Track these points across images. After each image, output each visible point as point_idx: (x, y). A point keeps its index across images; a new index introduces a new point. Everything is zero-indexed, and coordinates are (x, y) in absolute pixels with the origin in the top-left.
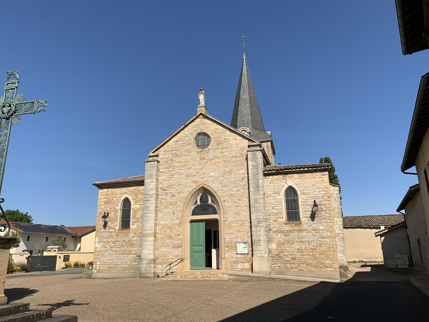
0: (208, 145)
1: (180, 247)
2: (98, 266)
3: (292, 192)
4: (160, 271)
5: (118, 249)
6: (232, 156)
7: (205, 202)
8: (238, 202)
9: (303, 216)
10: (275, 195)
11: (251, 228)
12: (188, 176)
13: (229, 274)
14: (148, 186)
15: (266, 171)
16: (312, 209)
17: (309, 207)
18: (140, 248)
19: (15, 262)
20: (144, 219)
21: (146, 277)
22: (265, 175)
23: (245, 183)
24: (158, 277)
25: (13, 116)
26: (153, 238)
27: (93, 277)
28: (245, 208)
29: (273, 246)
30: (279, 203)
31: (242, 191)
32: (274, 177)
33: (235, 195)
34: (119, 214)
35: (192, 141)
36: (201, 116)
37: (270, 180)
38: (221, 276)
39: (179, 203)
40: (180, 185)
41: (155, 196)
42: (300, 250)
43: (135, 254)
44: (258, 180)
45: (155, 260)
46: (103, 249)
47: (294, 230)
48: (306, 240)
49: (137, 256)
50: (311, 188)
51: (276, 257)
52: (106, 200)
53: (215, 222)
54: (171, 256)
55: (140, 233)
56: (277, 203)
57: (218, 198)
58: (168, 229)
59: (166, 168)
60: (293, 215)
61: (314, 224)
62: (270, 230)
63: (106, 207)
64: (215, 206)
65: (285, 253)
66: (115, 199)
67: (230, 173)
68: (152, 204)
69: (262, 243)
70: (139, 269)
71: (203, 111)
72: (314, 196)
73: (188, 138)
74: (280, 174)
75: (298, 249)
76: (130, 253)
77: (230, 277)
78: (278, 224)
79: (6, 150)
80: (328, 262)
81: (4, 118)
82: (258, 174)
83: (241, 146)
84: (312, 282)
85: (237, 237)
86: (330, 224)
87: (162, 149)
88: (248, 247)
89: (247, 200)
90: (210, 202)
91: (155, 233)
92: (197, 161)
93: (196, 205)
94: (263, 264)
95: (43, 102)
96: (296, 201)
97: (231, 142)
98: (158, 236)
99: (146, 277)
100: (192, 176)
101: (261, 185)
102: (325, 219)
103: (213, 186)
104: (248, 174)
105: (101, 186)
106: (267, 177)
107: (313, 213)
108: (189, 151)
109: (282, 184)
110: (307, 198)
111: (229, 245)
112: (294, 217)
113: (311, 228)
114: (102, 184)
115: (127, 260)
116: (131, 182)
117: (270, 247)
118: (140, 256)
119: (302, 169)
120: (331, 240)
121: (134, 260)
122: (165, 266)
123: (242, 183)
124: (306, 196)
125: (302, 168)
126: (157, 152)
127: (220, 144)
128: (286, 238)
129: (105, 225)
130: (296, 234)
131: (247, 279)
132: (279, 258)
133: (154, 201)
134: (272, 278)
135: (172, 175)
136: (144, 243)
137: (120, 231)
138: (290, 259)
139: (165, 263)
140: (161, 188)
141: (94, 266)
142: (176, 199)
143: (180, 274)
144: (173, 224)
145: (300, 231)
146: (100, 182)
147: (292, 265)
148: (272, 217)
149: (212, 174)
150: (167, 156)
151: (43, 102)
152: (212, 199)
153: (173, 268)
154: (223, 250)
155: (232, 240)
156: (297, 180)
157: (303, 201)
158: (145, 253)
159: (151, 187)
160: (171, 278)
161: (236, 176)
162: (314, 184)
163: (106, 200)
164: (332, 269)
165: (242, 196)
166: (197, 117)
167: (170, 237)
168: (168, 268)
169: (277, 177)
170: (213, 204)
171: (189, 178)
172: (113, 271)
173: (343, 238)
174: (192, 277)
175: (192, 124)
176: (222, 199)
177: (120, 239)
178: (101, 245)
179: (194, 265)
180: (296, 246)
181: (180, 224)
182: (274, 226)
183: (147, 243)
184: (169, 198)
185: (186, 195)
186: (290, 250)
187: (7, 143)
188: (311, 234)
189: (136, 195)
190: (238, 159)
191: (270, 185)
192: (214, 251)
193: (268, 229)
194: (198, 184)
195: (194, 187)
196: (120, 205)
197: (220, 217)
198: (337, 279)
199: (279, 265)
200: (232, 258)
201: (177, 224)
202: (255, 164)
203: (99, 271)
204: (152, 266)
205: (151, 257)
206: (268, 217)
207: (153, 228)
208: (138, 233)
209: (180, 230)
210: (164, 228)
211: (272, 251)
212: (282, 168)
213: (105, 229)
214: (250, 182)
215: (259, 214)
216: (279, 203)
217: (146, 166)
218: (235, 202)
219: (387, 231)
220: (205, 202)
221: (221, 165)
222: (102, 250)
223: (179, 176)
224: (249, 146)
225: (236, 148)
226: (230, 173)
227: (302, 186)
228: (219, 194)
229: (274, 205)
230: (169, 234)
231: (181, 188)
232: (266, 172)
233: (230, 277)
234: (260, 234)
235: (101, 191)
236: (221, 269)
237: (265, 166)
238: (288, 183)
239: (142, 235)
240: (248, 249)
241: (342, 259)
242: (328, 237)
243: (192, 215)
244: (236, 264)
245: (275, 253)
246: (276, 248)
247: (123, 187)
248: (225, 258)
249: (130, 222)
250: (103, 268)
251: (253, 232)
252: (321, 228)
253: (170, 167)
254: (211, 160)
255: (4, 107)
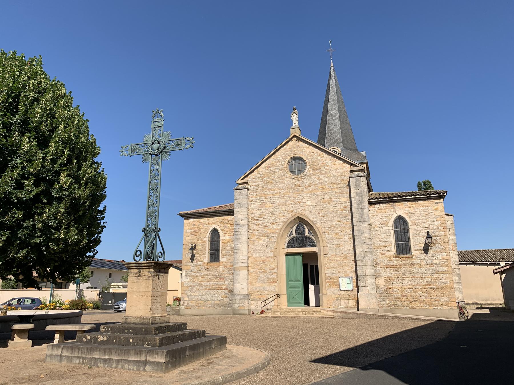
0: (303, 170)
1: (276, 282)
2: (186, 303)
3: (402, 222)
4: (254, 308)
5: (207, 284)
6: (332, 183)
7: (302, 233)
8: (340, 234)
9: (415, 248)
10: (382, 226)
11: (355, 262)
12: (281, 205)
13: (333, 311)
14: (239, 216)
15: (372, 199)
16: (425, 241)
17: (421, 238)
18: (231, 283)
19: (87, 298)
20: (236, 251)
21: (240, 314)
22: (370, 203)
23: (347, 213)
24: (253, 313)
25: (163, 153)
26: (245, 272)
27: (181, 313)
28: (348, 240)
29: (381, 282)
30: (388, 234)
31: (344, 221)
32: (381, 205)
33: (336, 226)
34: (207, 246)
35: (285, 166)
36: (294, 139)
37: (376, 209)
38: (325, 313)
39: (272, 235)
40: (273, 214)
41: (246, 226)
42: (411, 286)
43: (226, 289)
44: (363, 209)
45: (248, 296)
46: (191, 284)
47: (405, 264)
48: (418, 275)
49: (229, 292)
50: (424, 218)
51: (384, 294)
52: (192, 231)
53: (314, 255)
54: (266, 292)
55: (230, 266)
56: (385, 235)
57: (316, 230)
58: (262, 262)
59: (257, 196)
60: (403, 247)
61: (428, 258)
62: (377, 264)
63: (192, 238)
64: (313, 238)
65: (394, 290)
66: (202, 230)
67: (330, 201)
68: (243, 235)
69: (368, 278)
70: (231, 305)
71: (297, 133)
72: (426, 226)
73: (280, 163)
74: (388, 202)
75: (410, 285)
76: (220, 288)
77: (336, 314)
78: (386, 257)
79: (159, 183)
80: (444, 299)
81: (154, 154)
82: (362, 202)
83: (341, 171)
84: (428, 320)
85: (339, 272)
86: (446, 258)
87: (251, 176)
88: (353, 282)
89: (350, 231)
90: (307, 233)
91: (248, 267)
92: (291, 188)
93: (291, 237)
94: (370, 301)
95: (190, 139)
96: (406, 233)
97: (330, 167)
98: (251, 270)
99: (240, 314)
100: (285, 204)
101: (366, 215)
102: (440, 252)
103: (311, 216)
104: (351, 202)
105: (186, 216)
106: (373, 206)
107: (427, 245)
108: (282, 178)
109: (390, 213)
110: (419, 229)
111: (331, 280)
112: (404, 250)
113: (424, 262)
114: (188, 214)
115: (217, 296)
116: (219, 212)
117: (377, 283)
118: (231, 292)
119: (413, 197)
120: (447, 275)
121: (225, 296)
122: (260, 302)
123: (343, 213)
124: (418, 227)
125: (413, 195)
126: (246, 179)
127: (317, 169)
128: (396, 272)
129: (192, 258)
130: (407, 268)
131: (355, 316)
132: (387, 295)
133: (246, 233)
134: (383, 316)
135: (264, 204)
136: (236, 277)
137: (209, 264)
138: (400, 296)
139: (259, 299)
140: (252, 218)
141: (182, 302)
142: (269, 230)
143: (279, 310)
144: (267, 257)
145: (412, 265)
146: (186, 212)
147: (403, 303)
148: (378, 250)
149: (309, 203)
150: (258, 183)
151: (190, 139)
152: (309, 230)
153: (269, 305)
154: (324, 285)
155: (334, 275)
156: (407, 209)
157: (415, 232)
158: (238, 288)
159: (241, 216)
160: (270, 314)
161: (336, 205)
162: (427, 213)
163: (192, 231)
164: (449, 308)
165: (345, 227)
166: (291, 140)
167: (264, 271)
168: (263, 304)
169: (384, 205)
170: (310, 236)
171: (282, 207)
172: (202, 307)
173: (459, 274)
174: (293, 313)
175: (285, 147)
176: (322, 231)
177: (209, 272)
178: (188, 280)
179: (291, 301)
180: (407, 281)
181: (275, 257)
182: (382, 260)
183: (240, 277)
184: (261, 229)
185: (280, 225)
186: (400, 286)
187: (159, 177)
188: (424, 269)
189: (225, 226)
190: (339, 186)
191: (377, 214)
192: (311, 287)
193: (375, 263)
194: (293, 214)
195: (288, 217)
196: (207, 236)
197: (320, 250)
198: (455, 318)
199: (388, 302)
200: (335, 294)
201: (271, 257)
202: (358, 191)
203: (187, 308)
204: (246, 301)
205: (245, 292)
206: (374, 250)
207: (246, 261)
208: (228, 266)
209: (275, 263)
210: (256, 261)
211: (380, 287)
212: (390, 196)
213: (192, 262)
214: (353, 212)
215: (364, 247)
216: (388, 234)
217: (235, 194)
218: (336, 234)
219: (508, 267)
220: (302, 233)
221: (318, 193)
222: (189, 285)
223: (271, 205)
224: (351, 172)
225: (336, 174)
226: (330, 201)
227: (414, 215)
228: (318, 225)
229: (382, 237)
230: (262, 268)
231: (275, 219)
232: (372, 200)
233: (336, 314)
234: (366, 268)
235: (186, 221)
236: (322, 306)
237: (368, 193)
238: (397, 212)
239: (233, 269)
240: (353, 285)
241: (459, 297)
242: (444, 272)
243: (288, 247)
244: (339, 301)
245: (383, 289)
246: (384, 284)
247: (210, 217)
248: (326, 294)
249: (219, 254)
250: (191, 304)
251: (358, 267)
252: (436, 261)
253: (261, 195)
254: (307, 187)
255: (153, 143)
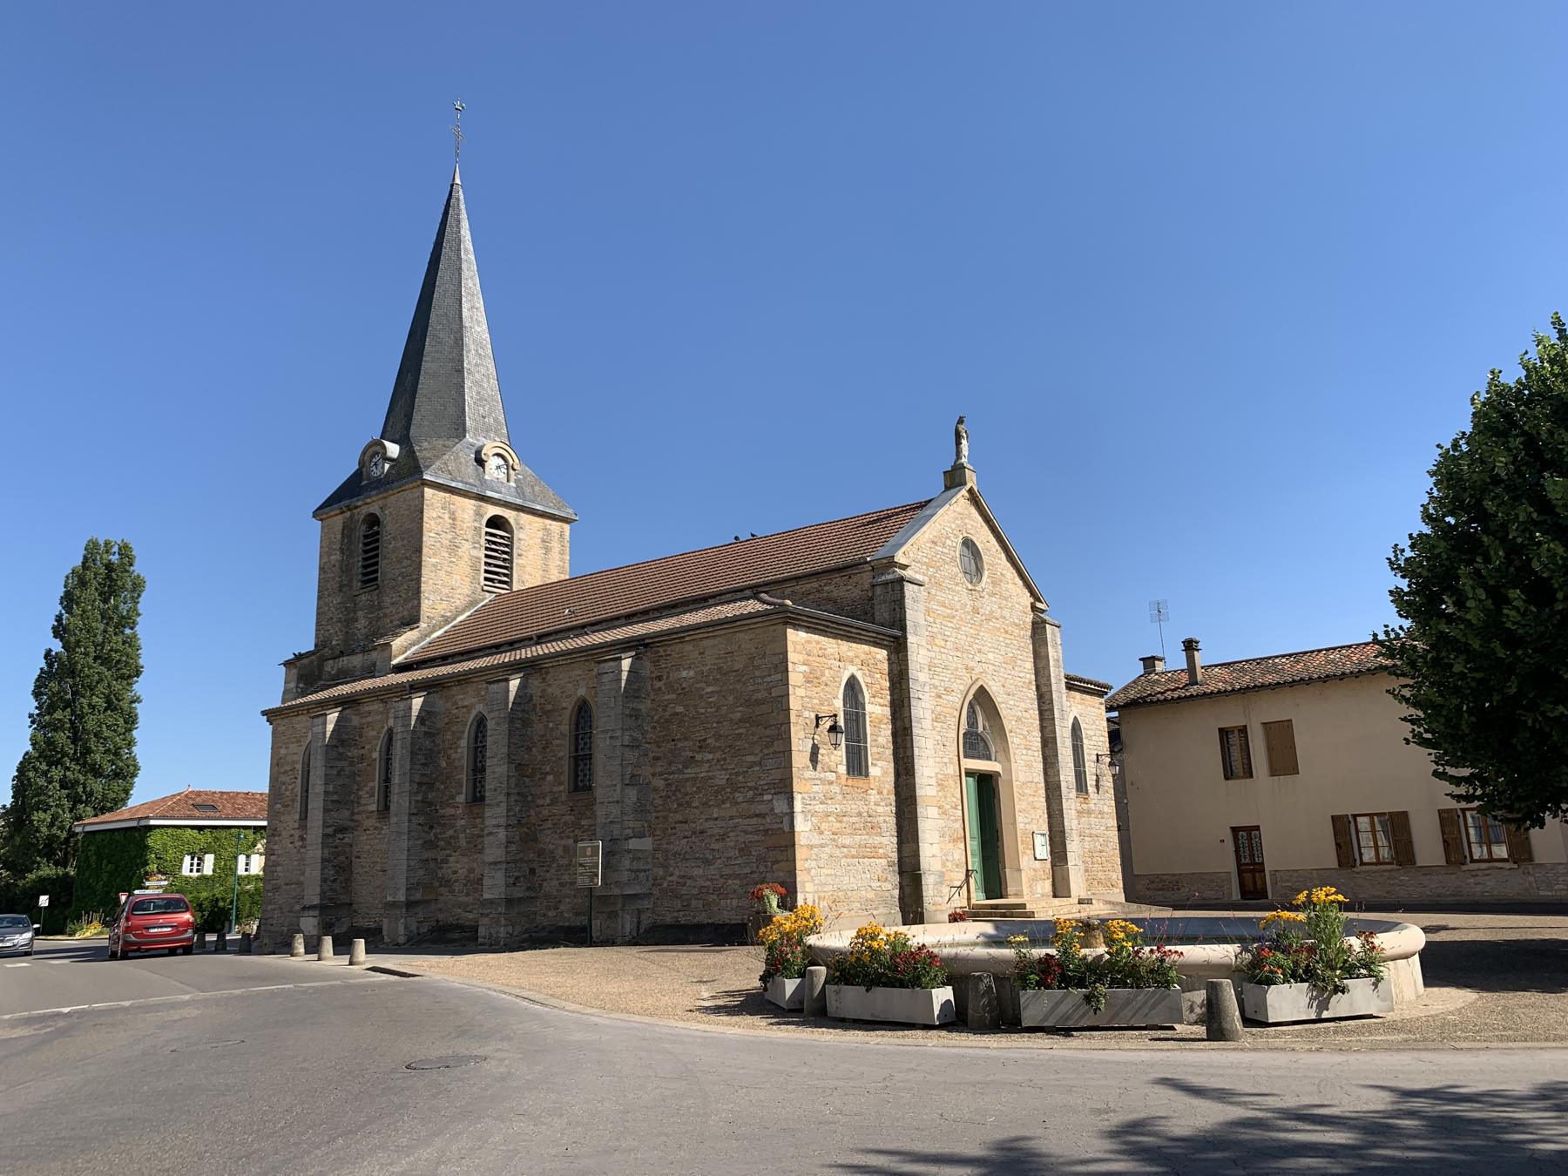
5: (847, 840)
40: (946, 668)
43: (885, 856)
46: (816, 839)
66: (827, 672)
103: (994, 689)
149: (991, 656)
196: (841, 696)
